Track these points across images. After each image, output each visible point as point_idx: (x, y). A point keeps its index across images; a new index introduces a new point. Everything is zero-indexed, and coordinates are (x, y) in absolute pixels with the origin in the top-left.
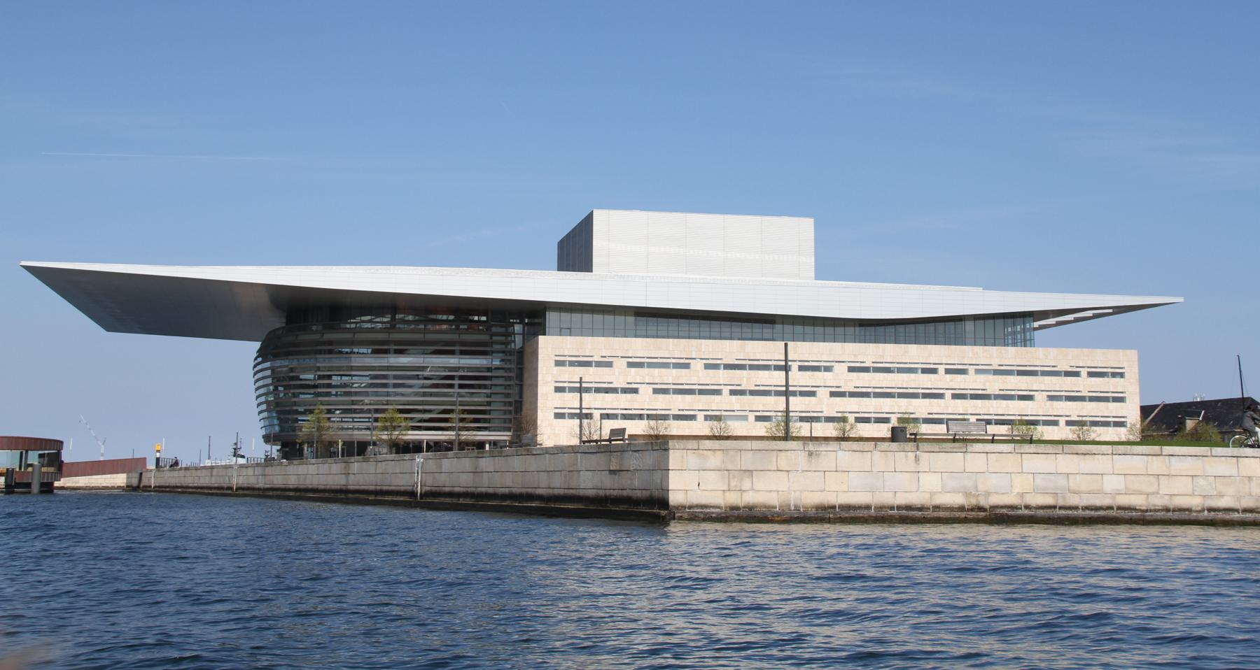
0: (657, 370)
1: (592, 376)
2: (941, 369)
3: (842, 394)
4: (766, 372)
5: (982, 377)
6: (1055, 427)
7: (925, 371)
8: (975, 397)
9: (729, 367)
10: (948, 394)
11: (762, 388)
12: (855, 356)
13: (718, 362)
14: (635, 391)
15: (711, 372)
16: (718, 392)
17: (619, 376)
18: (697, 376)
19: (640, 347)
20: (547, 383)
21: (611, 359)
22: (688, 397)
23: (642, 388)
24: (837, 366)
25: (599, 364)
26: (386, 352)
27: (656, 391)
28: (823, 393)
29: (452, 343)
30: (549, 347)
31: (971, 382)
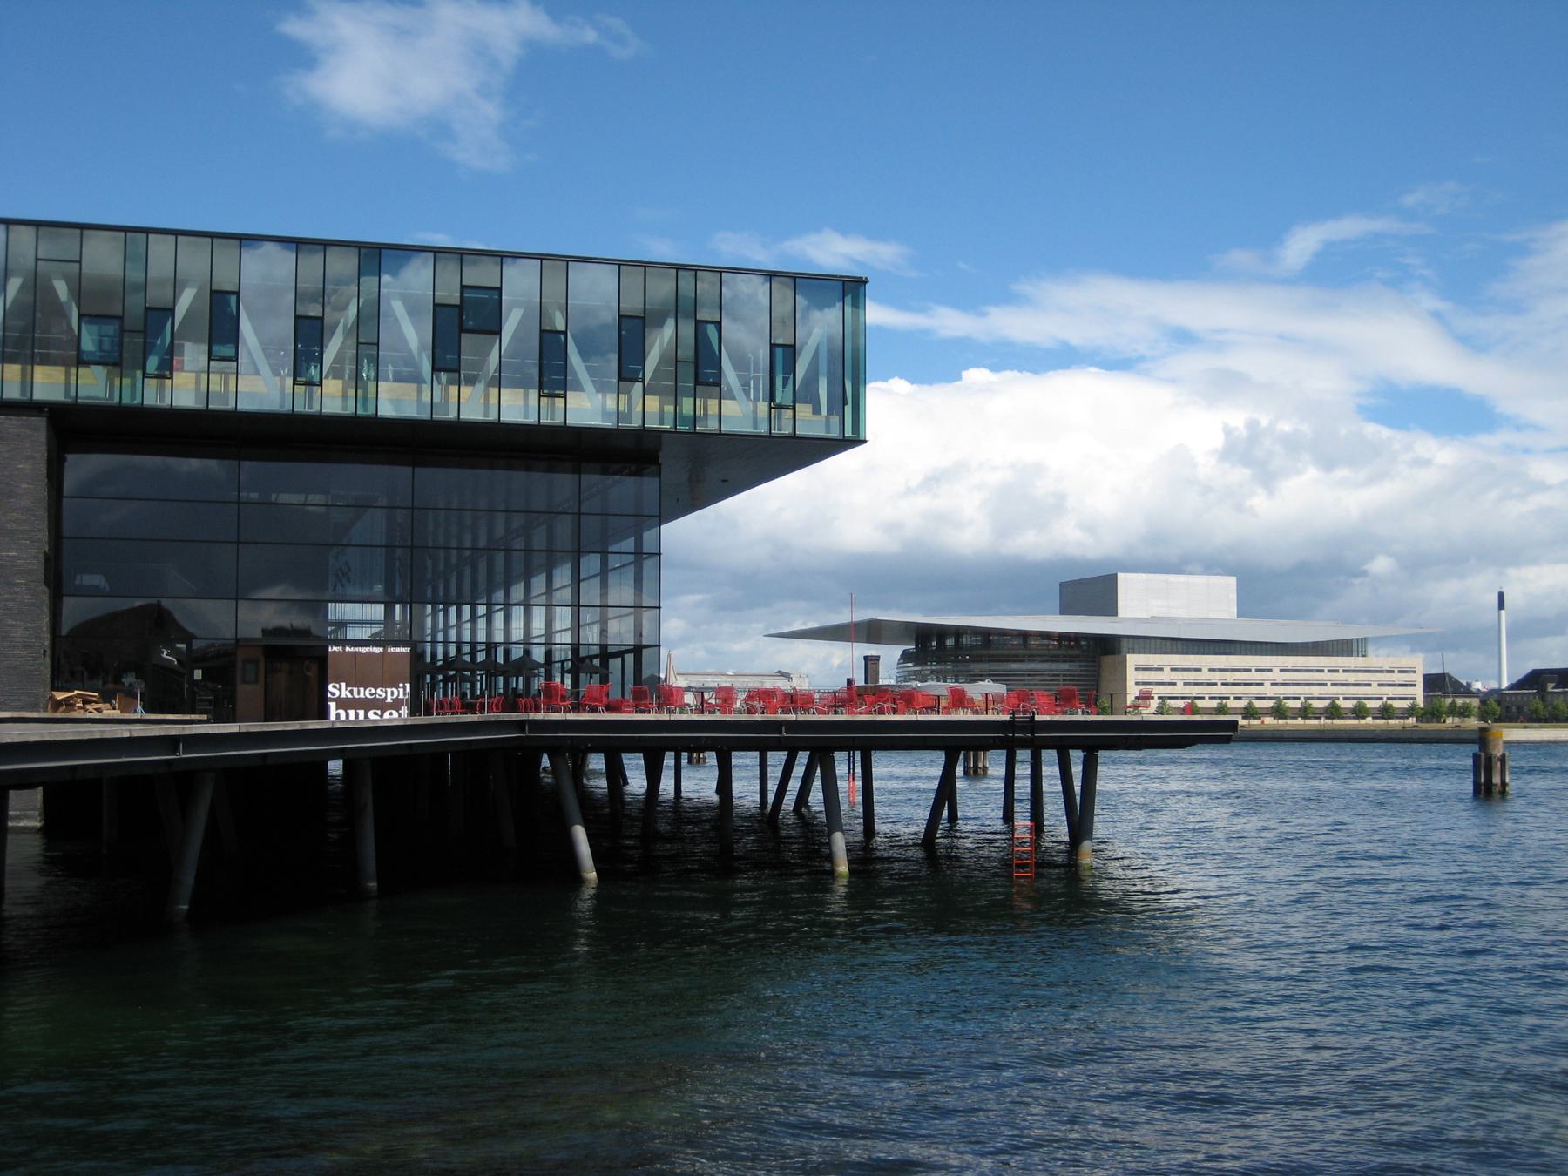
1: (1153, 676)
2: (1326, 670)
7: (1318, 671)
10: (1329, 683)
14: (1174, 684)
16: (1215, 684)
17: (1166, 676)
18: (1205, 676)
24: (1274, 669)
27: (1185, 684)
28: (1267, 684)
29: (1058, 656)
30: (1133, 660)
31: (1341, 677)
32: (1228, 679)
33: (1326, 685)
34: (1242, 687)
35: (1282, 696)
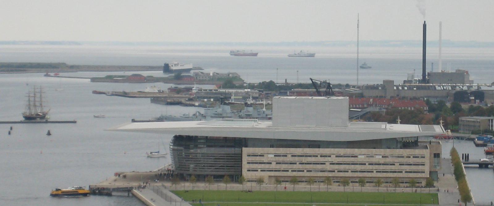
1: (258, 159)
3: (333, 164)
6: (401, 173)
9: (299, 156)
10: (367, 164)
11: (309, 162)
12: (338, 152)
14: (271, 163)
16: (296, 163)
18: (289, 159)
21: (263, 154)
22: (286, 165)
23: (273, 163)
24: (332, 156)
25: (260, 156)
27: (277, 163)
28: (328, 164)
32: (304, 160)
33: (365, 164)
34: (311, 166)
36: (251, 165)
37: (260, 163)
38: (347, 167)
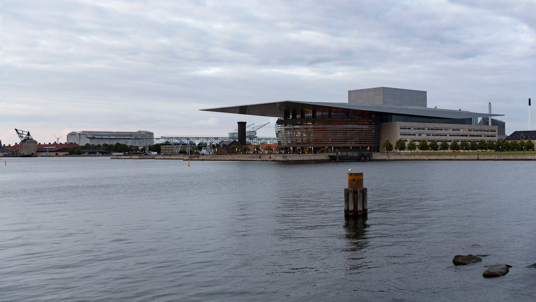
0: (419, 130)
1: (407, 131)
4: (438, 131)
5: (474, 132)
8: (473, 136)
9: (432, 129)
10: (469, 135)
13: (430, 128)
14: (415, 135)
15: (429, 130)
16: (429, 135)
17: (412, 131)
19: (416, 124)
20: (399, 133)
25: (409, 129)
26: (347, 124)
27: (419, 135)
28: (448, 135)
32: (435, 133)
34: (439, 137)
35: (436, 140)
36: (403, 136)
37: (409, 135)
38: (459, 138)
